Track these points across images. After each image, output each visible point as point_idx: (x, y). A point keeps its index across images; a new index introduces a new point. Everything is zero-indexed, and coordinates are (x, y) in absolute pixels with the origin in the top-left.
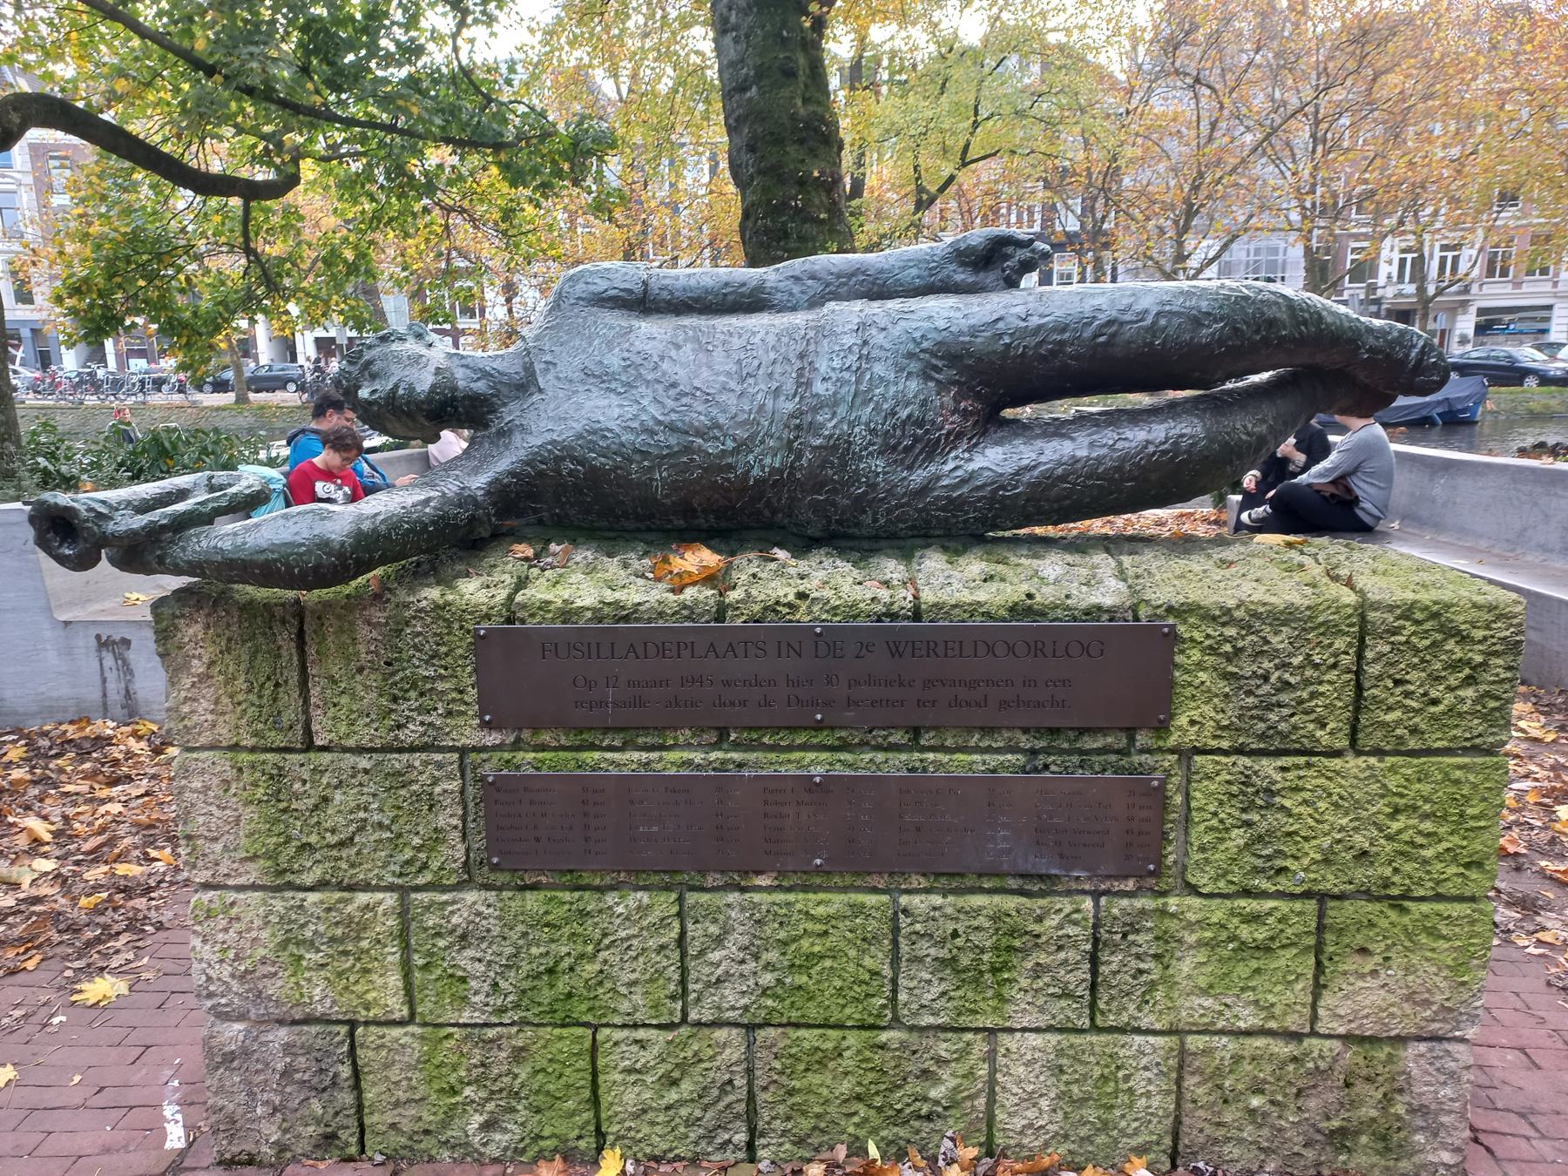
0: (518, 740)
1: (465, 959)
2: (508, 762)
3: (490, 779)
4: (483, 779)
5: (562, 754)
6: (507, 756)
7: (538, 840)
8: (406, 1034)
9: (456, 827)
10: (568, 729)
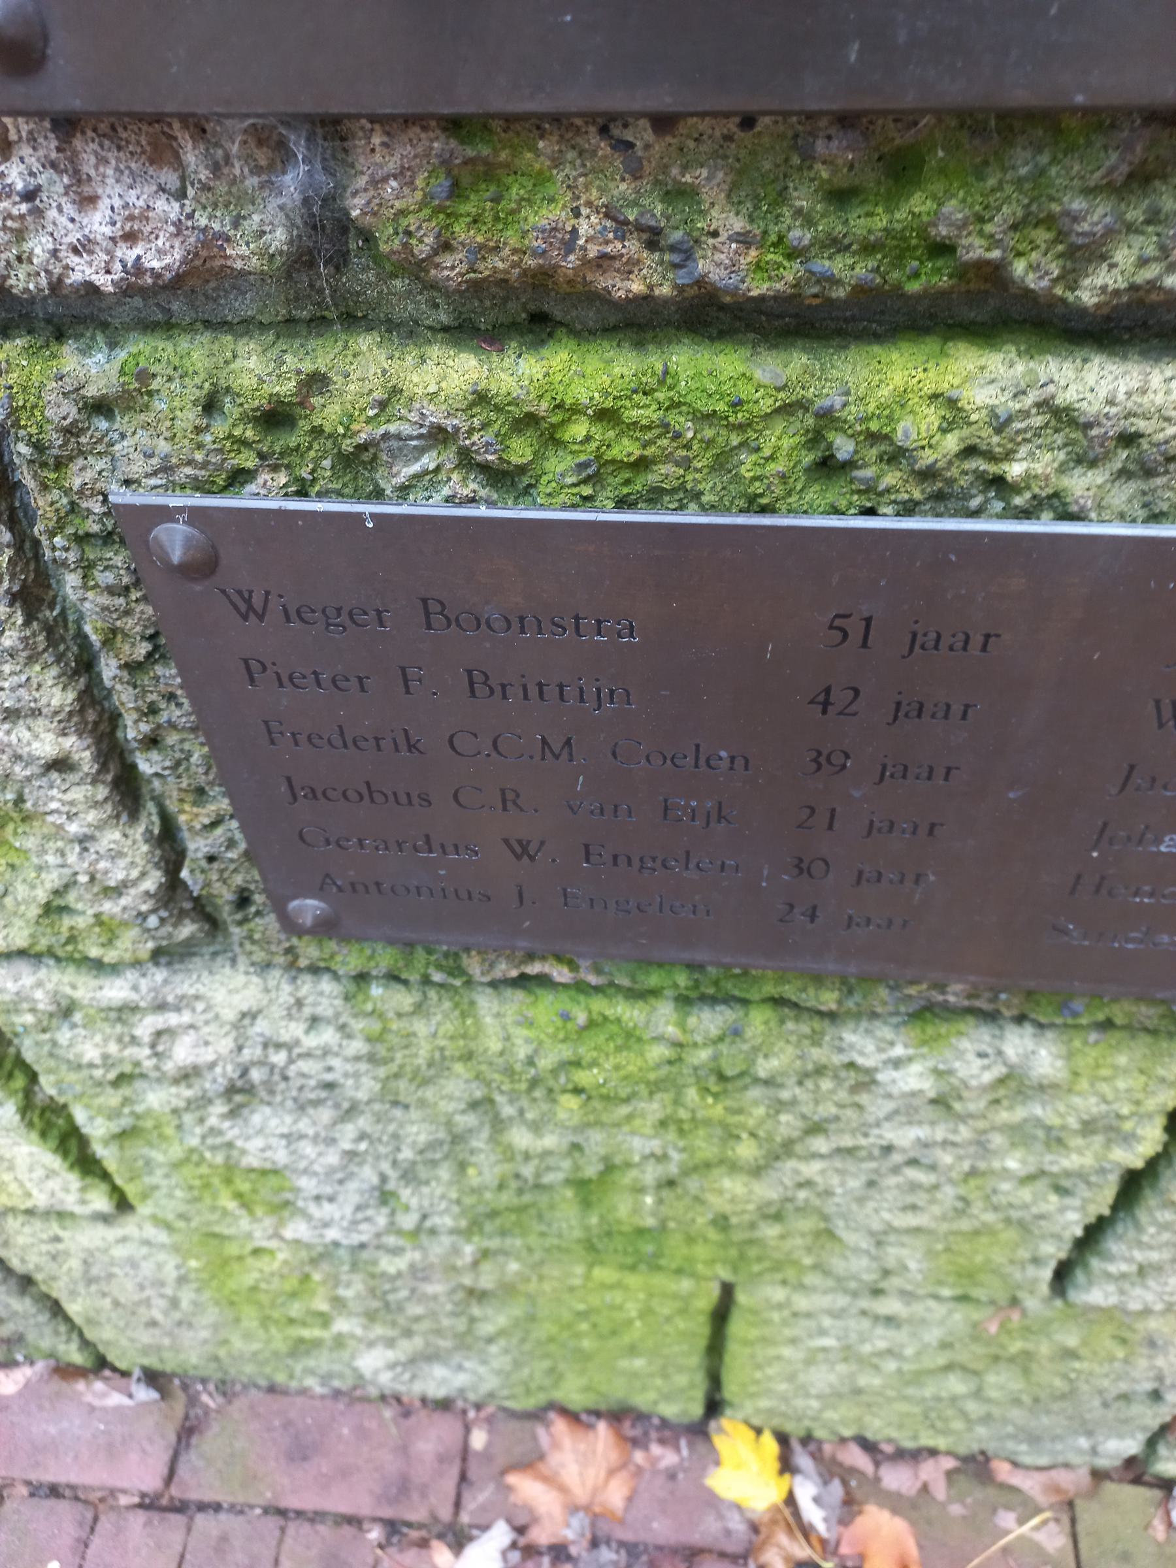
0: (329, 237)
1: (262, 1136)
2: (276, 417)
3: (175, 540)
4: (129, 528)
5: (707, 370)
6: (257, 369)
7: (522, 850)
8: (124, 1240)
9: (60, 764)
10: (764, 141)
